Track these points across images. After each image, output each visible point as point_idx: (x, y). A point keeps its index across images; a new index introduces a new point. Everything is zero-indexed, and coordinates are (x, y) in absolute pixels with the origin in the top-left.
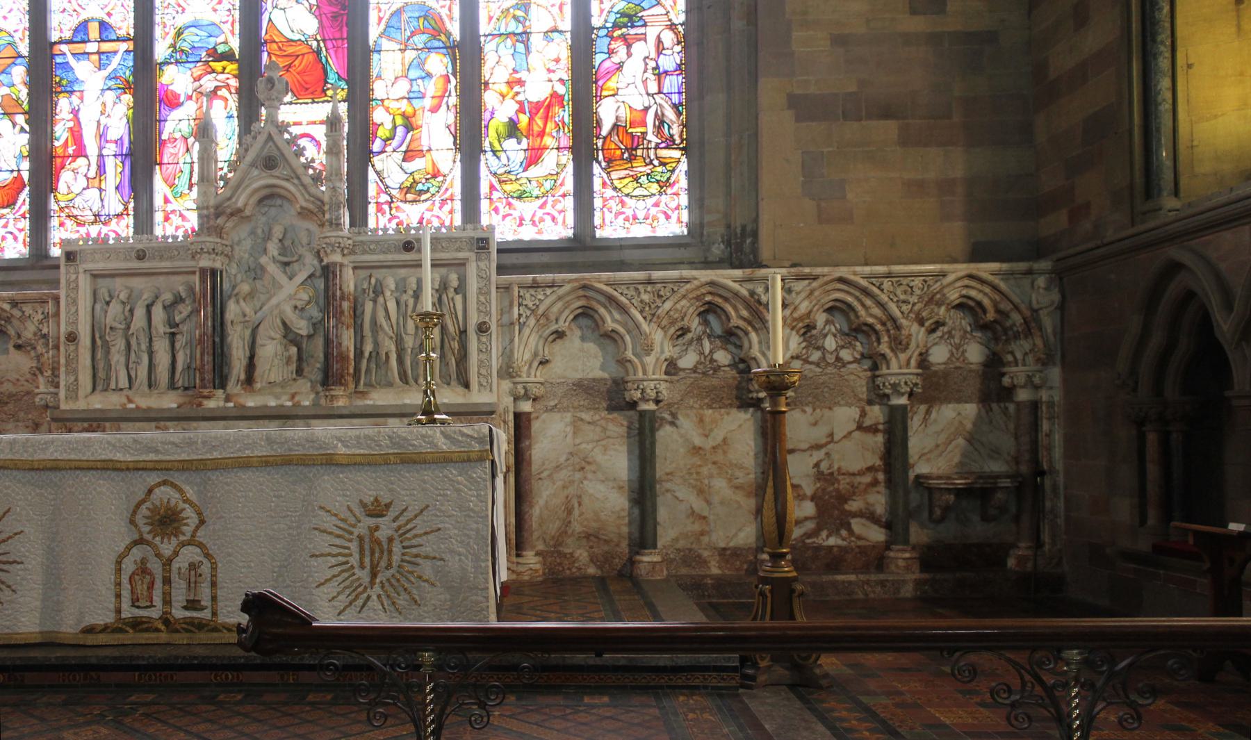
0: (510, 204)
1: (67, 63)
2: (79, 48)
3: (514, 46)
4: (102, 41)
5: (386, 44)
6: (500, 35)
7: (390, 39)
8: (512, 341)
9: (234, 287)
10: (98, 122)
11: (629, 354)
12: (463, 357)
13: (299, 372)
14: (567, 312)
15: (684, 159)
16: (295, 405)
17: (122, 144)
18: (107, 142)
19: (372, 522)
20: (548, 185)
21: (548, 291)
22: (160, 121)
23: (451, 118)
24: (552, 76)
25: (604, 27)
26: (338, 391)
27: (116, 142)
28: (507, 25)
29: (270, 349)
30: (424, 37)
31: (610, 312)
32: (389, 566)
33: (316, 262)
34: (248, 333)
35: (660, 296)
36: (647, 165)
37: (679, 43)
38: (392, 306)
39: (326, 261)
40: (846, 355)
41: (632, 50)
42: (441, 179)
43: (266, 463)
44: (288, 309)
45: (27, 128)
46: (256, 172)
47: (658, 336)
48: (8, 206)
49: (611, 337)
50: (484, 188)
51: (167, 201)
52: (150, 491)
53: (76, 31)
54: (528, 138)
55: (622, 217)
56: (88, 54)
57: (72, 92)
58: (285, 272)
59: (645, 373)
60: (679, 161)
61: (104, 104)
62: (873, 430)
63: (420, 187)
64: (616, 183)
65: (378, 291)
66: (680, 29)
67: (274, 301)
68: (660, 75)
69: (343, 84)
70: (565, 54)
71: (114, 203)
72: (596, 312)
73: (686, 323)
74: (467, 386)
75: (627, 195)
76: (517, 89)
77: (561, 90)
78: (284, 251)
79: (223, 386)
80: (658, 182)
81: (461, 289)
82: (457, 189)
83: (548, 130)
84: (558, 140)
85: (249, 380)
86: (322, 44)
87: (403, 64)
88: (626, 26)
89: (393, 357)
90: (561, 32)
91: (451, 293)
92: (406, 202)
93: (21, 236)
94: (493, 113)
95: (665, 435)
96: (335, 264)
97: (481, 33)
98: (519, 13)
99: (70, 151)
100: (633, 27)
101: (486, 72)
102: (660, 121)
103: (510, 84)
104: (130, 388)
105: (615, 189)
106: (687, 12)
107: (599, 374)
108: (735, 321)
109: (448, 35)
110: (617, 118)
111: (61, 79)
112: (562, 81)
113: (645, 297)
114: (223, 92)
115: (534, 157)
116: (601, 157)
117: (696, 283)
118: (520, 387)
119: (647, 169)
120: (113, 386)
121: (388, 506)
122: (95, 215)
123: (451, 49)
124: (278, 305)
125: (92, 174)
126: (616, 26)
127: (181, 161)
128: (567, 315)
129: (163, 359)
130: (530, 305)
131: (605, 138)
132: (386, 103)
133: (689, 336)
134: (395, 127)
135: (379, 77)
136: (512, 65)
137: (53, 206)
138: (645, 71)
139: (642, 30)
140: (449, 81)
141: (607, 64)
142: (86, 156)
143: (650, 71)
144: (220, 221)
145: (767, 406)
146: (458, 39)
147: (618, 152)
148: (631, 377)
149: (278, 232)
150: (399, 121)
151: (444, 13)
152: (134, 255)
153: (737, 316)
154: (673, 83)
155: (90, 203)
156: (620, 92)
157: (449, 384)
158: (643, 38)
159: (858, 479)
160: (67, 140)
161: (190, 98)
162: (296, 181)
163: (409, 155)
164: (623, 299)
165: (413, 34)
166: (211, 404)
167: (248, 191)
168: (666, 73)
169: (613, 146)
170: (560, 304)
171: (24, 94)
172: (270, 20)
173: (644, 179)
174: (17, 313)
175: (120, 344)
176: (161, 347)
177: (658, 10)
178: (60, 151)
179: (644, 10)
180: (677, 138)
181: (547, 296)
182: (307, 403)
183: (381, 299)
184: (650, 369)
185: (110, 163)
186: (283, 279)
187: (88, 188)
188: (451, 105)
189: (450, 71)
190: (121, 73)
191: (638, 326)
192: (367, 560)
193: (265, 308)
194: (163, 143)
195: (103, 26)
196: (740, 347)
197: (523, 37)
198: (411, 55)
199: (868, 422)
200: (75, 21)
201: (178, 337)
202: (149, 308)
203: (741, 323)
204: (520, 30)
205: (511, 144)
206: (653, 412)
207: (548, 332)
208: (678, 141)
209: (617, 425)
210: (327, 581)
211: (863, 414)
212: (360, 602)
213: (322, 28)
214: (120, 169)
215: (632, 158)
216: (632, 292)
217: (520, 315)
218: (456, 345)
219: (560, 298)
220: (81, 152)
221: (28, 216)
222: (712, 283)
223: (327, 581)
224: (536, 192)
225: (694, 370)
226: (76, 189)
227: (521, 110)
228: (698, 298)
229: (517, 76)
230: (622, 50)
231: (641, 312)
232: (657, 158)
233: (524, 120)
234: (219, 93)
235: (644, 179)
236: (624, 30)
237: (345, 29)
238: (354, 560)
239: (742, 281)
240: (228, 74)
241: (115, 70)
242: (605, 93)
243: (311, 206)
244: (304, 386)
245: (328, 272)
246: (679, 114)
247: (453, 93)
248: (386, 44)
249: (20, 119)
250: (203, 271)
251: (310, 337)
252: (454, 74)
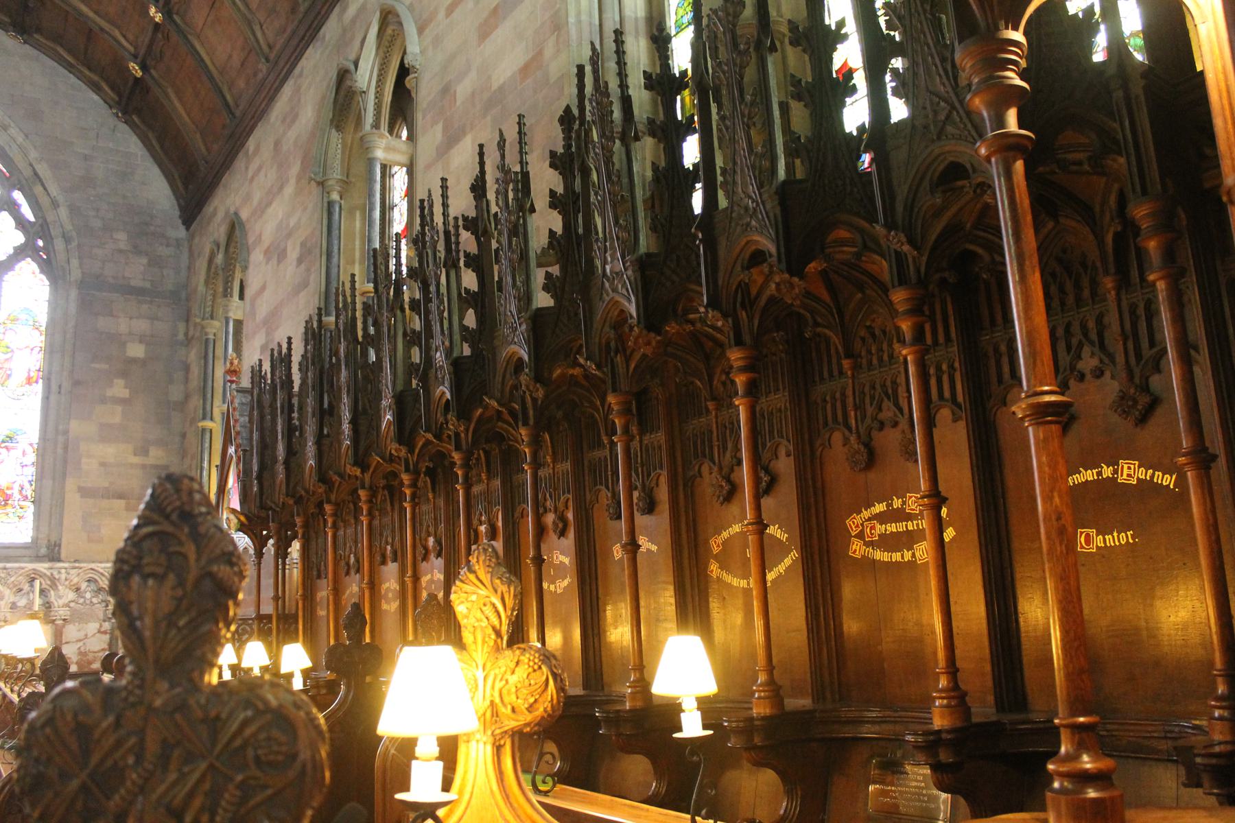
40: (95, 600)
62: (105, 633)
73: (21, 587)
119: (14, 510)
159: (96, 655)
199: (103, 629)
211: (101, 626)
215: (6, 504)
225: (25, 607)
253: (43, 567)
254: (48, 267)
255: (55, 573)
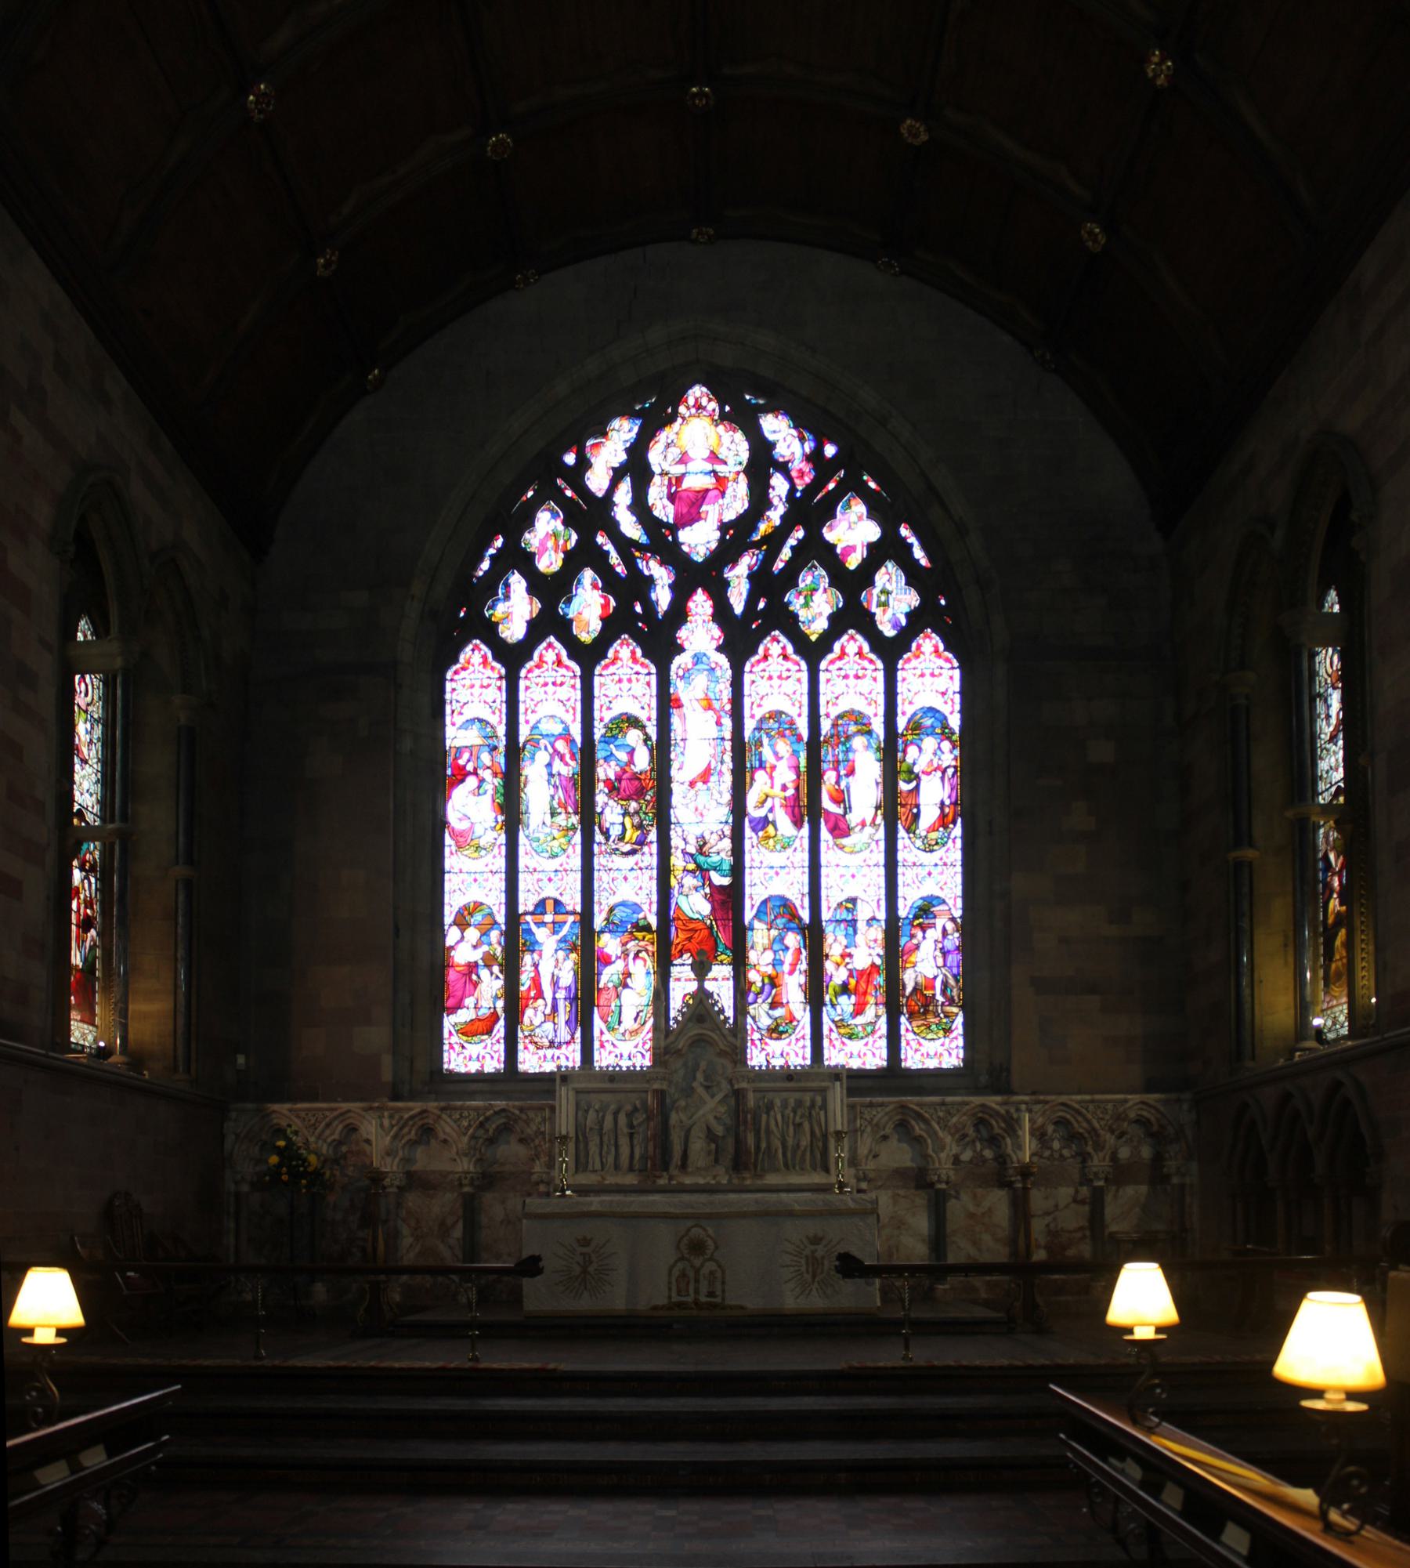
0: (843, 1043)
1: (530, 929)
2: (539, 918)
3: (846, 929)
4: (555, 914)
5: (757, 924)
6: (837, 921)
7: (760, 920)
8: (856, 1142)
9: (674, 1102)
10: (553, 975)
11: (930, 1151)
12: (825, 1152)
13: (716, 1161)
14: (890, 1123)
15: (961, 1014)
16: (718, 1183)
17: (570, 991)
18: (559, 988)
19: (812, 1247)
20: (869, 1029)
21: (879, 1109)
22: (598, 974)
23: (802, 979)
24: (871, 951)
25: (907, 918)
26: (746, 1175)
27: (566, 988)
28: (841, 914)
29: (698, 1145)
30: (784, 920)
31: (918, 1124)
32: (822, 1272)
33: (729, 1087)
34: (683, 1134)
35: (950, 1114)
36: (936, 1017)
37: (958, 931)
38: (779, 1117)
39: (736, 1087)
41: (926, 935)
42: (795, 1023)
43: (756, 1215)
44: (711, 1118)
45: (501, 976)
46: (690, 1025)
47: (948, 1139)
48: (487, 1034)
49: (919, 1140)
50: (826, 1031)
51: (602, 1033)
52: (689, 1230)
53: (537, 906)
54: (855, 994)
55: (919, 1053)
56: (546, 923)
57: (533, 951)
58: (708, 1092)
59: (940, 1162)
60: (957, 1015)
61: (557, 960)
63: (781, 1029)
64: (915, 1029)
65: (770, 1107)
66: (959, 921)
67: (701, 1112)
68: (945, 953)
69: (728, 952)
70: (880, 936)
71: (564, 1034)
72: (909, 1123)
74: (827, 1170)
75: (923, 1038)
76: (847, 960)
77: (878, 962)
78: (707, 1078)
79: (666, 1169)
80: (943, 1029)
81: (824, 1107)
82: (808, 1031)
83: (869, 991)
84: (876, 998)
85: (684, 1166)
86: (714, 923)
87: (769, 939)
88: (922, 917)
89: (780, 1151)
90: (878, 921)
91: (817, 1109)
92: (771, 1038)
93: (496, 1056)
94: (831, 977)
95: (952, 1204)
96: (743, 1089)
97: (823, 918)
98: (850, 906)
99: (532, 994)
100: (927, 918)
101: (826, 950)
102: (945, 984)
103: (843, 956)
104: (602, 1170)
105: (915, 1033)
106: (964, 909)
107: (909, 1164)
108: (997, 1130)
109: (801, 919)
110: (916, 983)
111: (526, 941)
112: (878, 955)
113: (941, 1114)
114: (643, 954)
115: (859, 1010)
116: (905, 1011)
117: (973, 1105)
118: (861, 1172)
119: (936, 1020)
120: (590, 1167)
121: (821, 1239)
122: (550, 1042)
123: (802, 929)
124: (704, 1115)
125: (548, 1011)
126: (916, 917)
127: (613, 1005)
128: (891, 1125)
129: (625, 1151)
130: (868, 1118)
131: (908, 998)
132: (757, 967)
133: (968, 1139)
134: (764, 985)
135: (752, 948)
136: (844, 942)
137: (520, 1034)
138: (935, 949)
139: (932, 921)
140: (801, 953)
141: (909, 945)
142: (544, 999)
143: (938, 950)
144: (667, 1057)
145: (1019, 1185)
146: (807, 922)
147: (917, 1008)
148: (931, 1167)
149: (703, 1065)
150: (766, 981)
151: (798, 904)
152: (606, 1078)
153: (998, 1127)
154: (954, 959)
155: (546, 1033)
156: (918, 964)
157: (815, 1170)
158: (933, 926)
160: (530, 987)
161: (618, 958)
162: (718, 1032)
163: (774, 1005)
164: (927, 1115)
165: (776, 918)
166: (662, 1182)
167: (686, 1037)
168: (949, 952)
169: (913, 1003)
170: (886, 1118)
171: (499, 951)
172: (677, 903)
173: (933, 1027)
174: (524, 1116)
175: (597, 1140)
176: (624, 1142)
177: (943, 907)
178: (525, 995)
179: (934, 906)
180: (956, 998)
181: (878, 1112)
182: (725, 1182)
183: (772, 1113)
184: (943, 1161)
185: (561, 1004)
186: (706, 1096)
187: (545, 1021)
188: (802, 970)
189: (802, 945)
190: (569, 938)
191: (936, 1133)
192: (810, 1269)
193: (694, 1118)
194: (599, 990)
195: (557, 903)
196: (999, 1147)
197: (853, 923)
198: (774, 933)
200: (535, 899)
201: (635, 1135)
202: (616, 1114)
203: (1000, 1131)
204: (850, 917)
205: (843, 999)
206: (944, 1190)
207: (878, 1136)
208: (957, 1001)
209: (921, 1199)
210: (789, 1280)
212: (807, 1292)
213: (713, 910)
214: (568, 1009)
215: (926, 1012)
216: (932, 1111)
217: (861, 1125)
218: (820, 1144)
219: (887, 1114)
220: (540, 995)
221: (502, 1041)
222: (983, 1105)
223: (789, 1280)
224: (861, 1035)
225: (971, 1162)
226: (537, 1022)
227: (851, 975)
228: (974, 1115)
229: (848, 951)
230: (920, 934)
231: (938, 1123)
232: (943, 1012)
233: (853, 982)
234: (640, 955)
235: (933, 1027)
236: (921, 920)
237: (730, 912)
238: (803, 1269)
239: (1005, 1103)
240: (651, 945)
241: (565, 936)
242: (908, 965)
243: (728, 1049)
244: (720, 1170)
245: (739, 1095)
246: (957, 981)
247: (804, 962)
248: (757, 924)
249: (496, 969)
250: (656, 1091)
251: (724, 1137)
252: (805, 947)
253: (993, 1101)
254: (954, 643)
255: (1012, 1110)
